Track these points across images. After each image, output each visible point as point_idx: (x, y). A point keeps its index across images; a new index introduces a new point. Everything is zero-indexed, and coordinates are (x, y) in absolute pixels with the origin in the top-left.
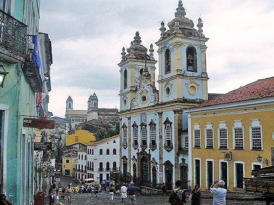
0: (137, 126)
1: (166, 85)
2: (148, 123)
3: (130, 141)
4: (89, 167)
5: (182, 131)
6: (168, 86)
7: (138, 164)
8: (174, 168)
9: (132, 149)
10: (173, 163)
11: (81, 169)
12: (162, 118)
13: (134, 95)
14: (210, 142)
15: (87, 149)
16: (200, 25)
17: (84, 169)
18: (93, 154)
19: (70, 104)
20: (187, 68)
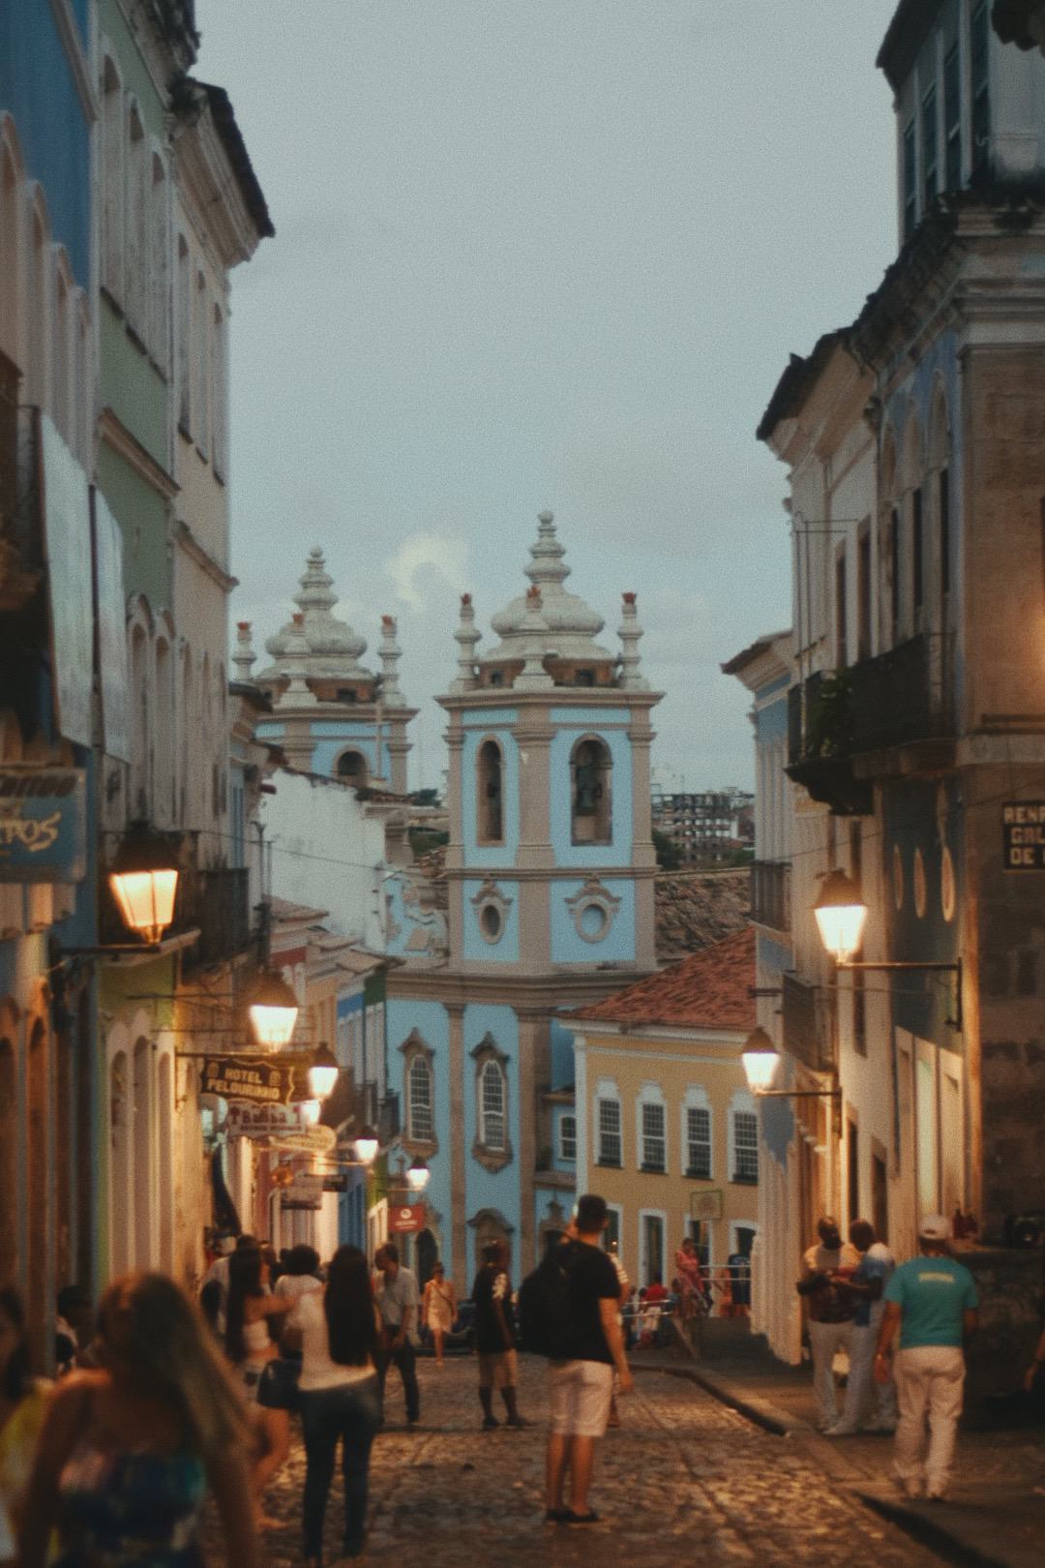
1: (483, 895)
6: (496, 902)
10: (513, 1215)
12: (461, 1029)
16: (629, 637)
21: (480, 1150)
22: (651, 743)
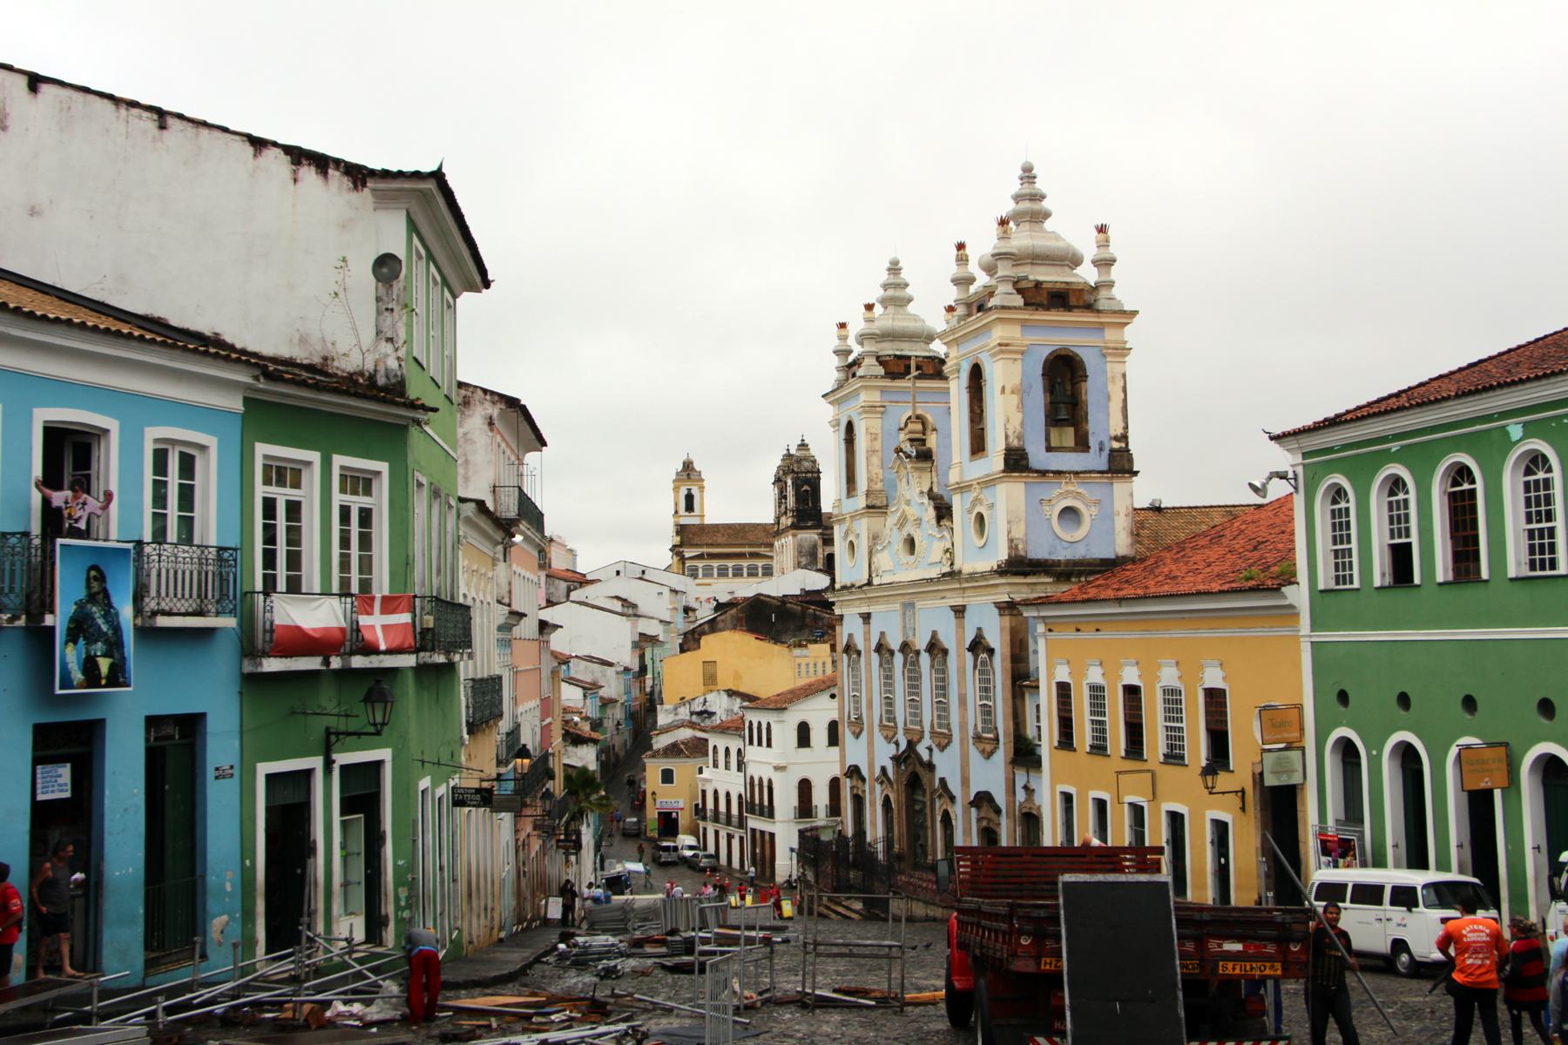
0: (892, 653)
2: (921, 643)
4: (757, 802)
5: (1022, 680)
7: (898, 802)
8: (1004, 821)
9: (879, 738)
10: (1000, 799)
11: (722, 808)
13: (876, 522)
14: (1099, 729)
15: (747, 725)
16: (1105, 263)
17: (735, 811)
18: (769, 745)
19: (689, 499)
20: (1048, 439)
21: (978, 738)
22: (1127, 359)
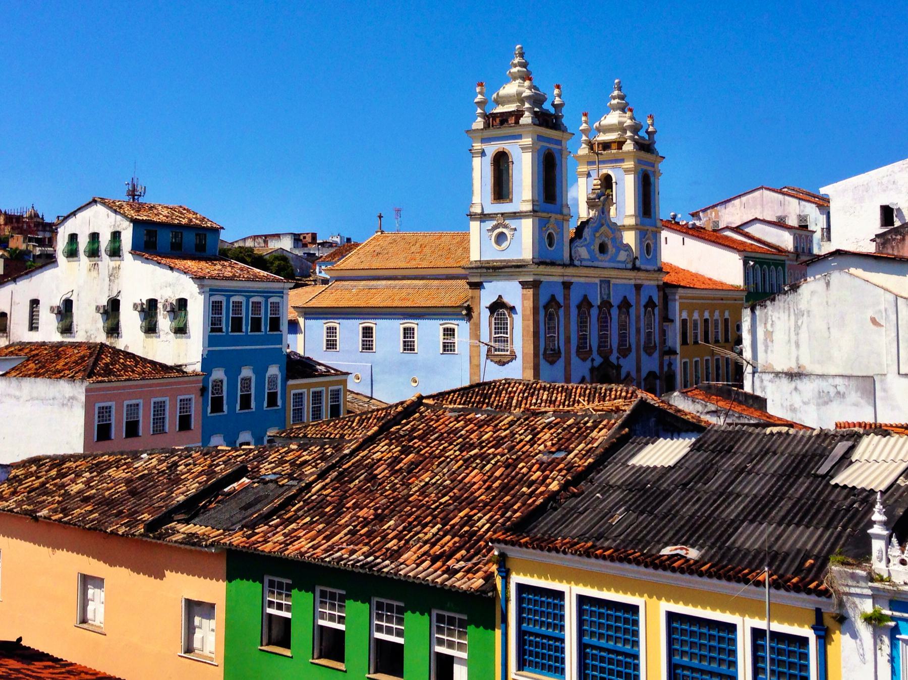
3: (568, 340)
12: (640, 295)
